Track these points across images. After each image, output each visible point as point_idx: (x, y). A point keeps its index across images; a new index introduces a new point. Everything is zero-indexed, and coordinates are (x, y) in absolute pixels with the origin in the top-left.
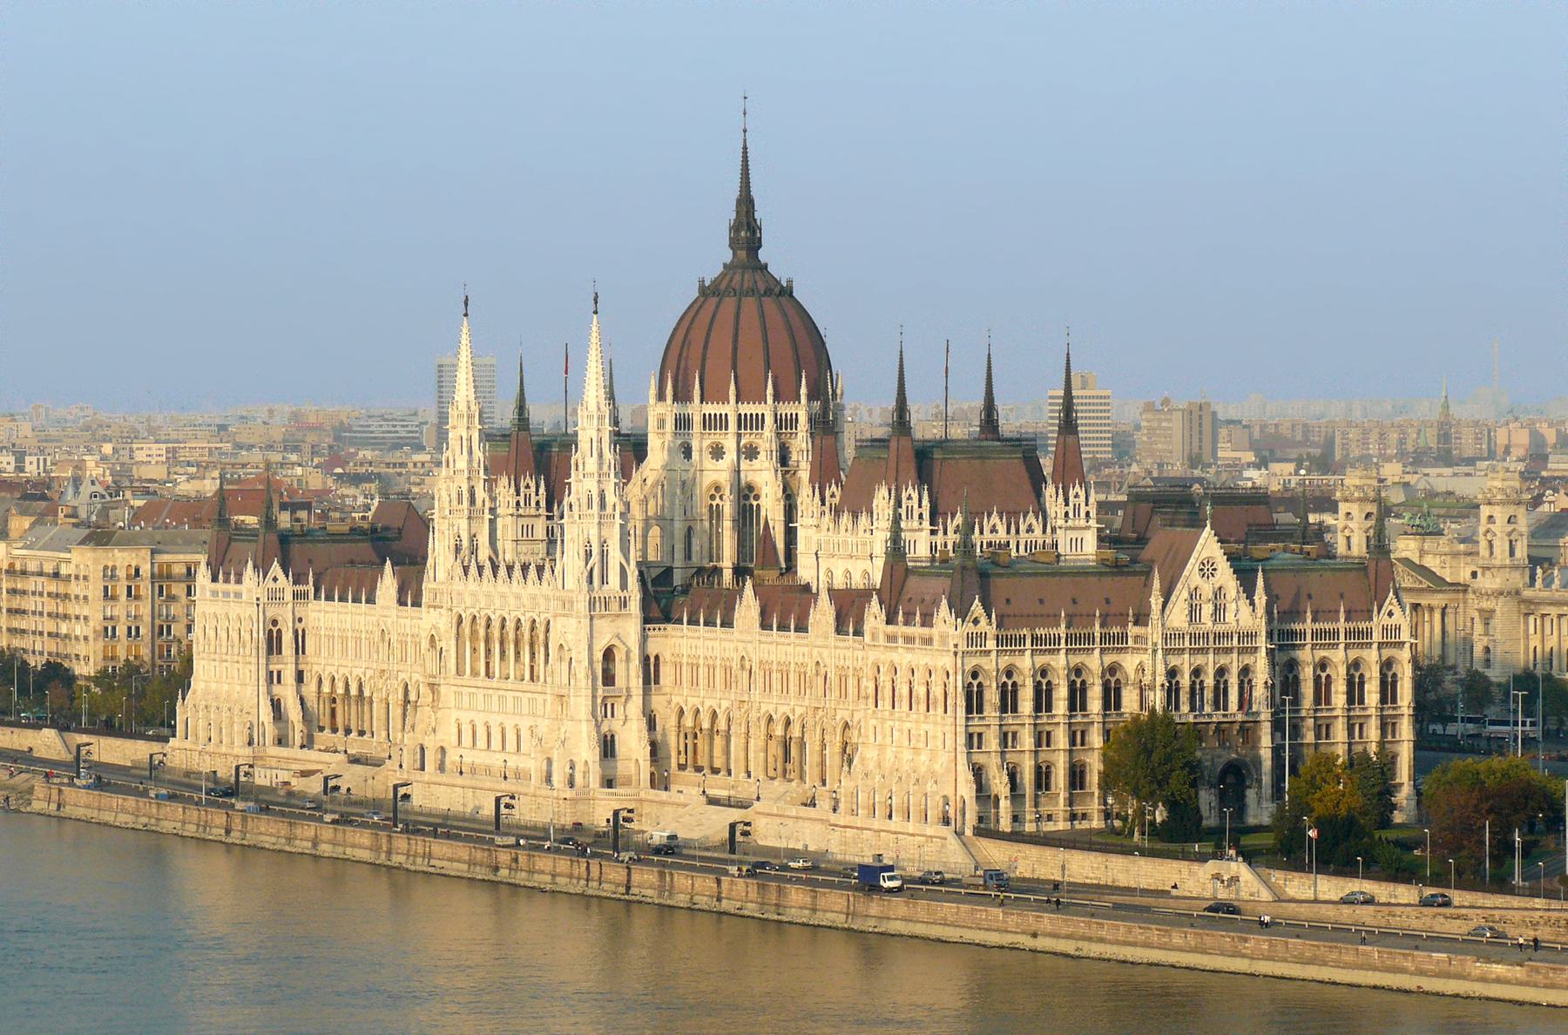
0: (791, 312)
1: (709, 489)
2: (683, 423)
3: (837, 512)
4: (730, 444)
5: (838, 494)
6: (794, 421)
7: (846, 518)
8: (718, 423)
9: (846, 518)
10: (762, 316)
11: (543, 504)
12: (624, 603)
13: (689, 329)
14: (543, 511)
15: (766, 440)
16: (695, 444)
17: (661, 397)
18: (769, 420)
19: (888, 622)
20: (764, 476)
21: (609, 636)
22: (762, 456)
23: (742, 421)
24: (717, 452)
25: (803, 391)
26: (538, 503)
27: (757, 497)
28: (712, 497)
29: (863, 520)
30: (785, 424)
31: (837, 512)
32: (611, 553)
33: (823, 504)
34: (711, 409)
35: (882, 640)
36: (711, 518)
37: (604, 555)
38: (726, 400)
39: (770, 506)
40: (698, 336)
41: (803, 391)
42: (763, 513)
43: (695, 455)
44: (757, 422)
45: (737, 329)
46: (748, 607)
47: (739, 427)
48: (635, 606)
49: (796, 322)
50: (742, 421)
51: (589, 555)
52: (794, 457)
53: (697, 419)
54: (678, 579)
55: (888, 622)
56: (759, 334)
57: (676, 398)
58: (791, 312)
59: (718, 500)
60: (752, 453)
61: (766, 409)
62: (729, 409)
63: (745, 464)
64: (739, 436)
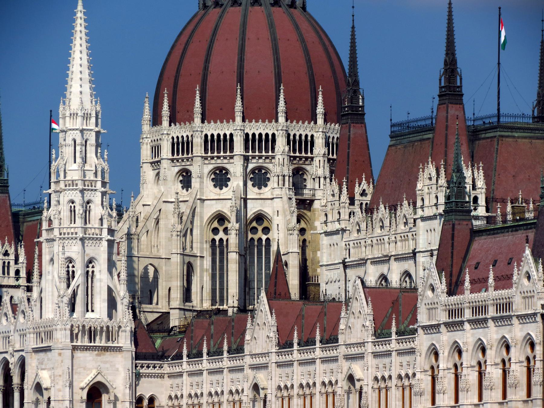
0: (304, 26)
1: (211, 221)
2: (182, 146)
3: (369, 210)
4: (236, 168)
5: (370, 190)
6: (307, 144)
7: (382, 211)
8: (224, 143)
9: (382, 211)
10: (271, 26)
11: (23, 274)
12: (109, 334)
13: (187, 44)
14: (23, 282)
15: (279, 164)
16: (195, 169)
17: (156, 121)
18: (281, 144)
19: (451, 293)
20: (275, 202)
21: (94, 372)
22: (273, 183)
23: (250, 141)
24: (221, 178)
25: (320, 109)
26: (17, 272)
27: (266, 230)
28: (215, 231)
29: (405, 209)
30: (301, 146)
31: (369, 210)
32: (97, 275)
33: (352, 203)
34: (215, 129)
35: (443, 317)
36: (213, 254)
37: (89, 276)
38: (231, 118)
39: (283, 237)
40: (198, 47)
41: (320, 109)
42: (274, 248)
43: (195, 183)
44: (269, 142)
45: (243, 39)
46: (262, 332)
47: (246, 149)
48: (125, 340)
49: (310, 36)
50: (250, 141)
51: (70, 276)
52: (309, 184)
53: (198, 142)
54: (175, 321)
55: (451, 293)
56: (269, 44)
57: (173, 120)
58: (304, 26)
59: (221, 235)
60: (259, 178)
61: (278, 128)
62: (236, 128)
63: (253, 192)
64: (246, 159)
